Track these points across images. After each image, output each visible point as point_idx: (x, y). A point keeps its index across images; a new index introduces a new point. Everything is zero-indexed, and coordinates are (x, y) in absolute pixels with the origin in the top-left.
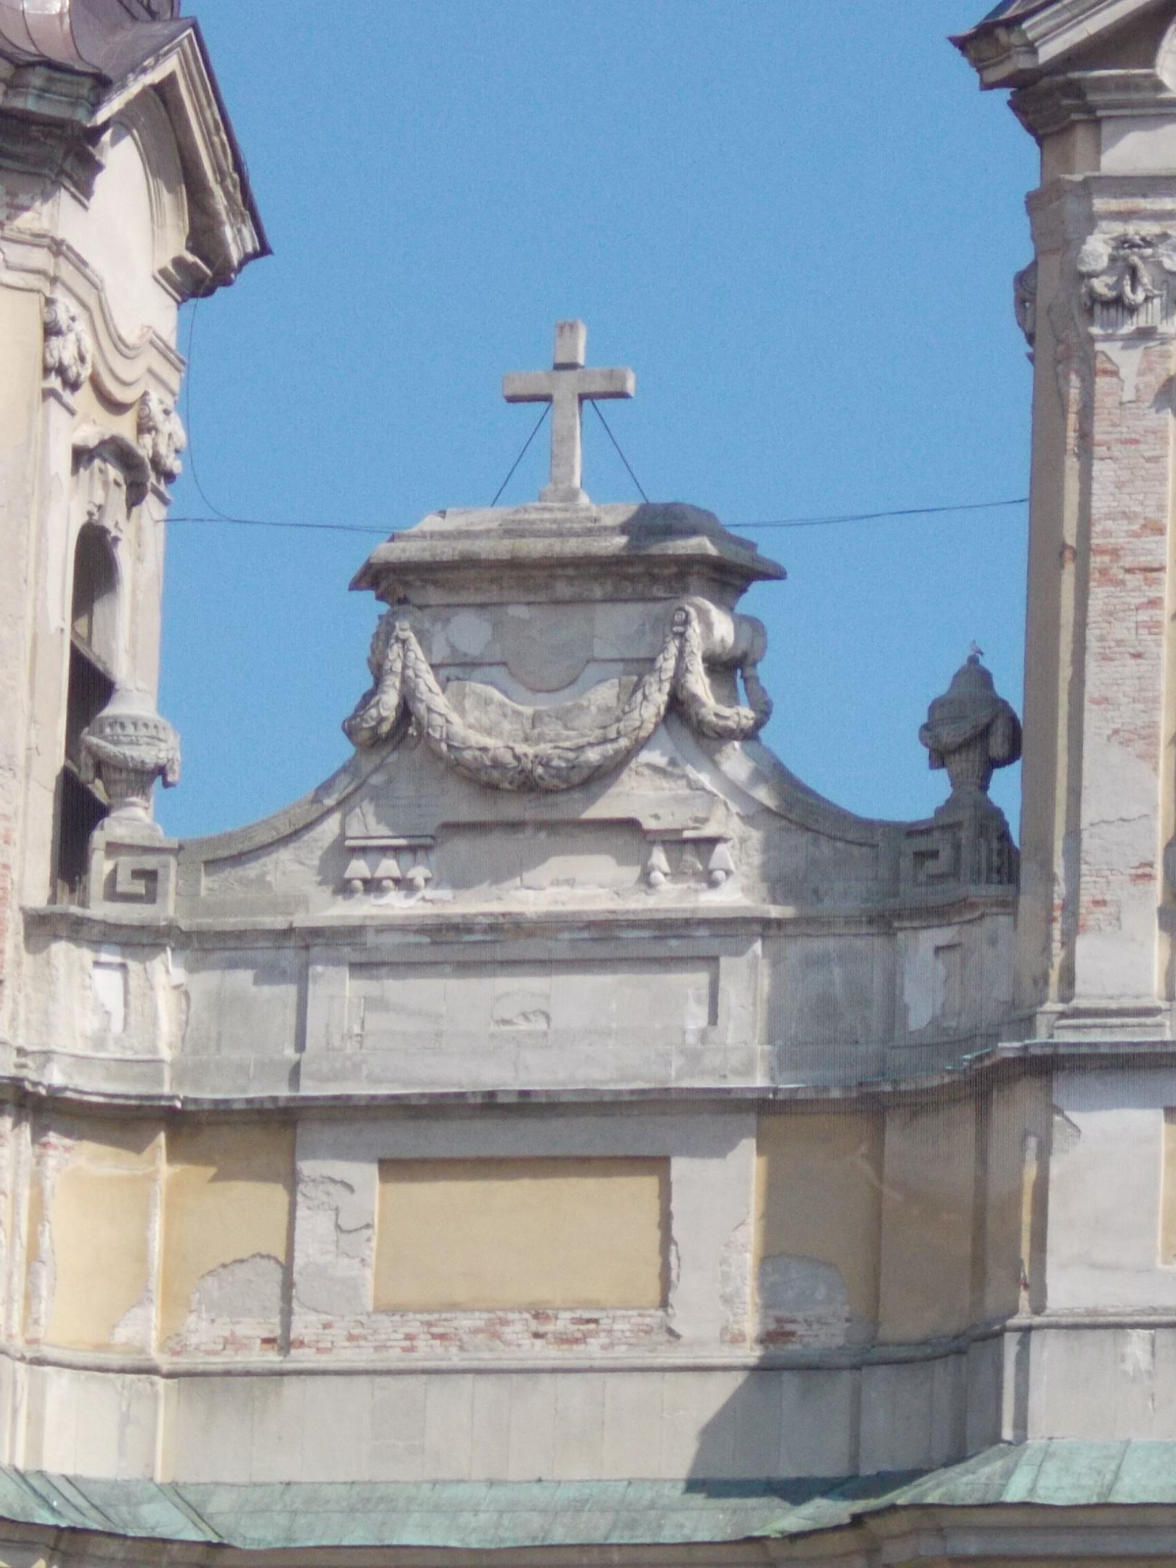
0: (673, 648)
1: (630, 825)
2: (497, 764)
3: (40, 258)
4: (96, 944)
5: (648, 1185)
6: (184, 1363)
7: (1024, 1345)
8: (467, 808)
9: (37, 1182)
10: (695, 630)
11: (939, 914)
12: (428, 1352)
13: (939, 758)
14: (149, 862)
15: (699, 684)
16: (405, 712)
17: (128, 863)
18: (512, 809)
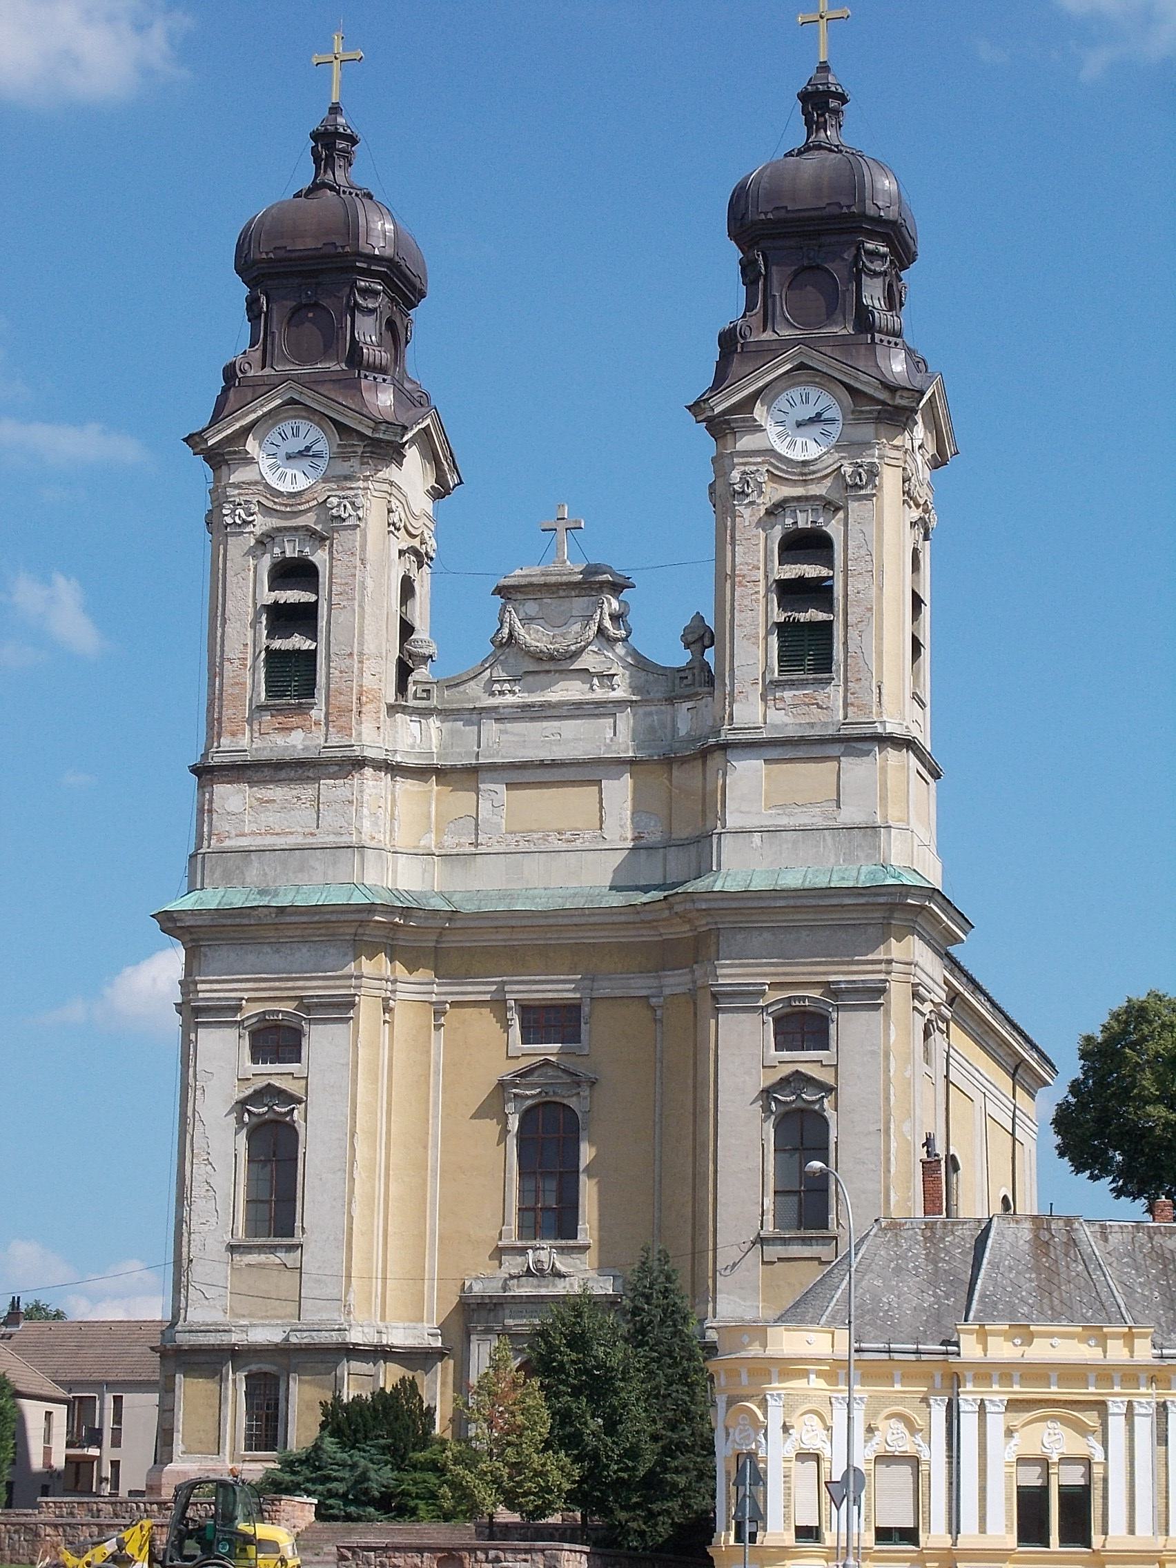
0: (599, 612)
2: (541, 651)
3: (386, 487)
4: (410, 715)
5: (596, 788)
6: (443, 852)
7: (719, 839)
9: (393, 793)
10: (606, 605)
11: (689, 698)
12: (523, 846)
13: (687, 646)
14: (427, 687)
15: (607, 623)
16: (511, 635)
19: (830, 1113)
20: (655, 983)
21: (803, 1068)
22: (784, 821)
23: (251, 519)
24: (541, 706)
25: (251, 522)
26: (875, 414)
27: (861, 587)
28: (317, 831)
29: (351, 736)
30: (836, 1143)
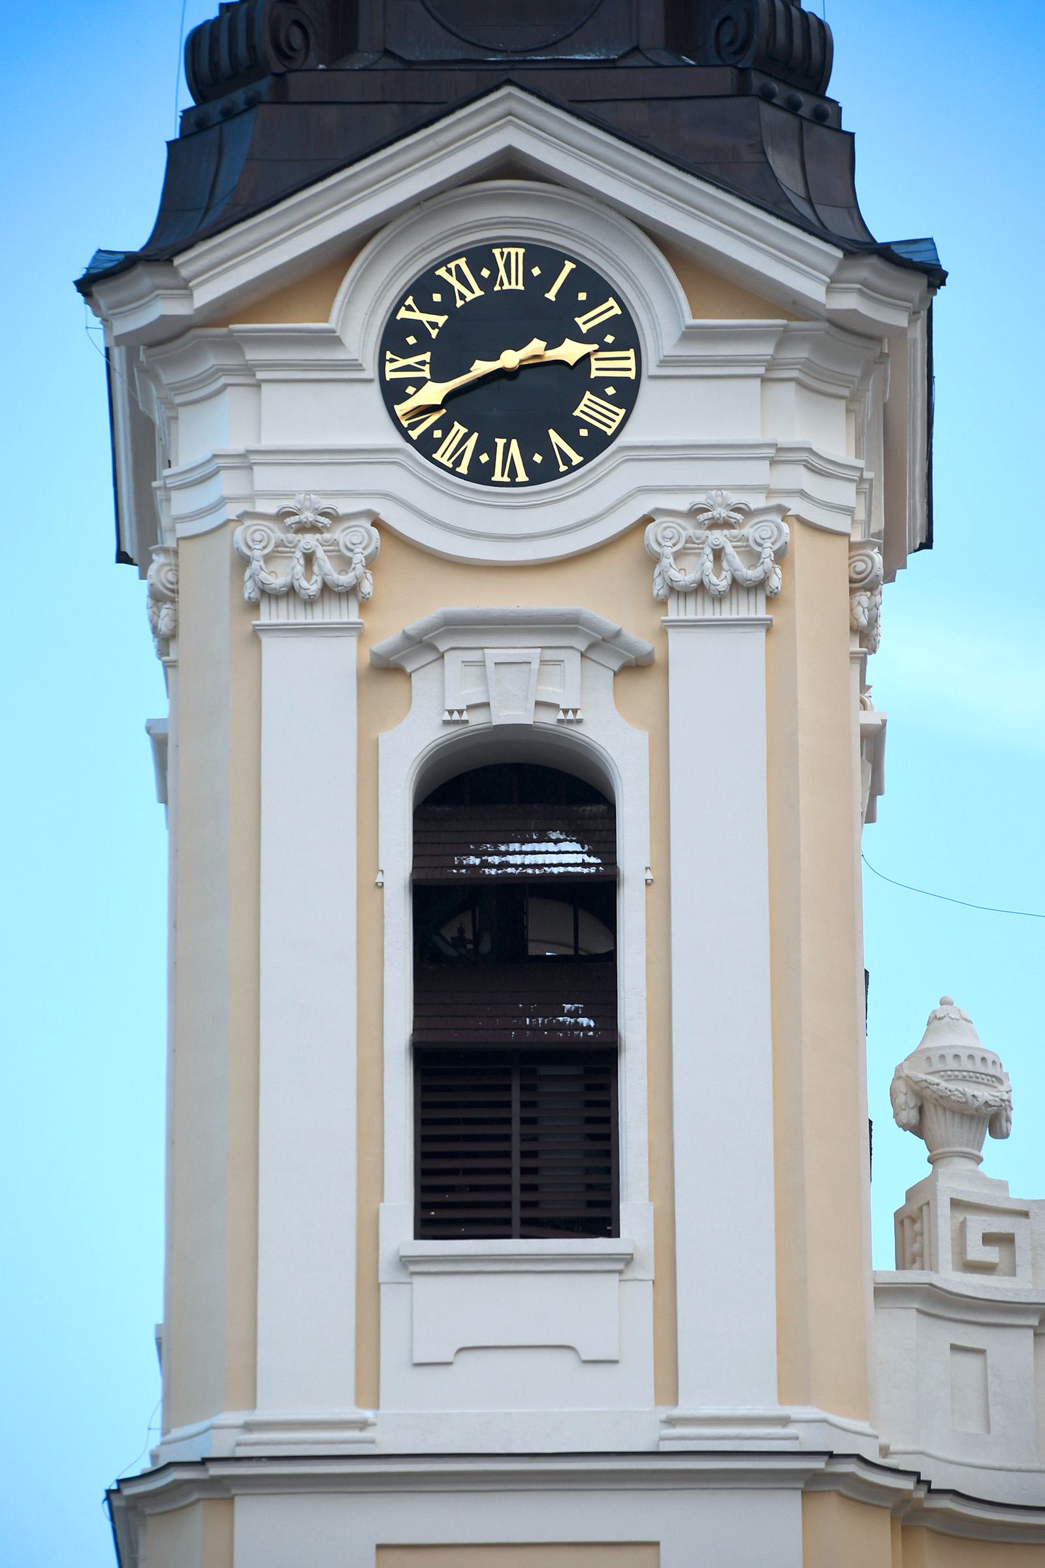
17: (978, 1224)
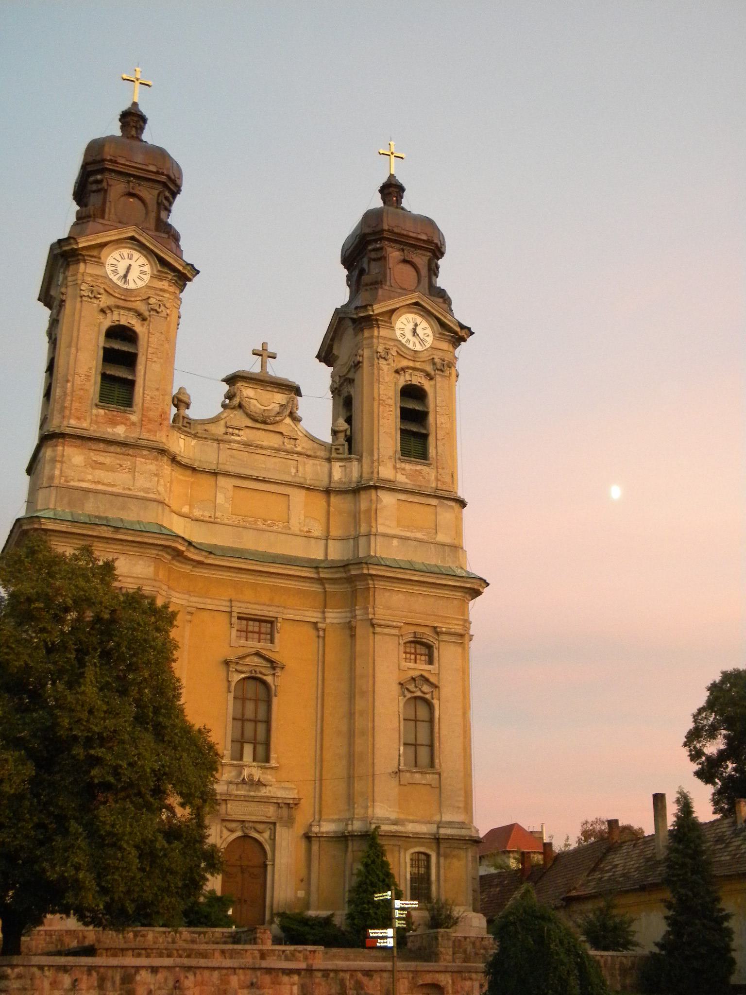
1: (281, 433)
8: (250, 423)
18: (258, 425)
19: (435, 702)
20: (320, 615)
21: (425, 674)
22: (408, 534)
23: (99, 296)
24: (256, 447)
25: (98, 298)
26: (449, 338)
27: (443, 422)
28: (132, 488)
29: (156, 436)
30: (439, 719)
